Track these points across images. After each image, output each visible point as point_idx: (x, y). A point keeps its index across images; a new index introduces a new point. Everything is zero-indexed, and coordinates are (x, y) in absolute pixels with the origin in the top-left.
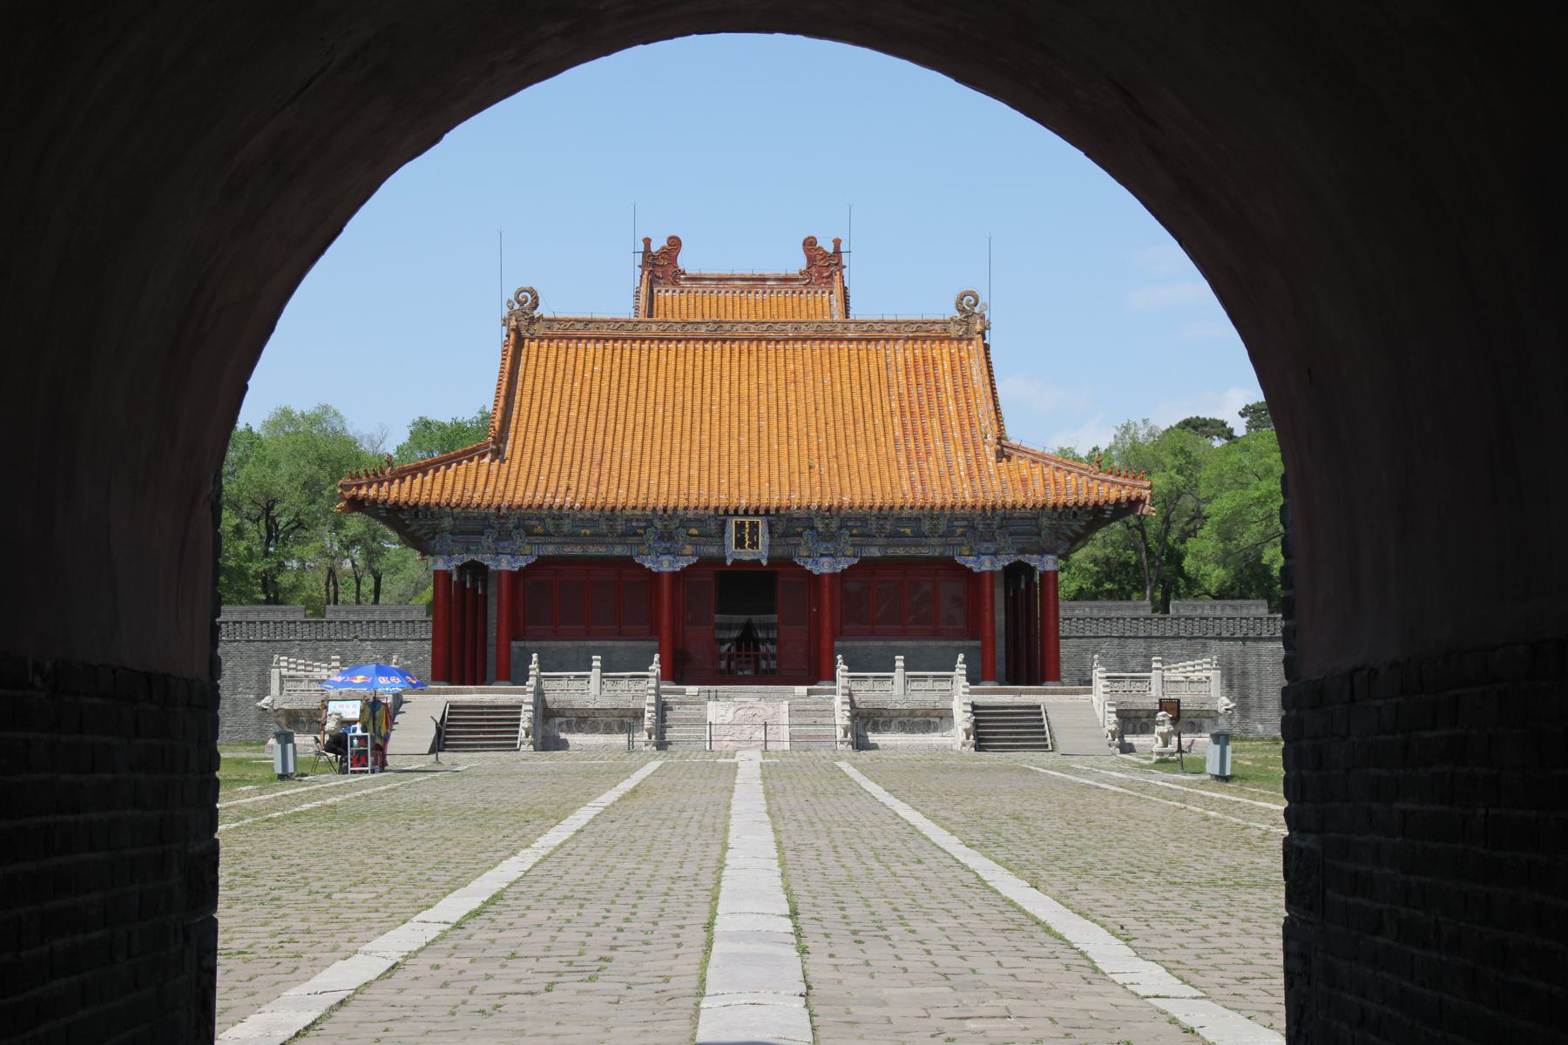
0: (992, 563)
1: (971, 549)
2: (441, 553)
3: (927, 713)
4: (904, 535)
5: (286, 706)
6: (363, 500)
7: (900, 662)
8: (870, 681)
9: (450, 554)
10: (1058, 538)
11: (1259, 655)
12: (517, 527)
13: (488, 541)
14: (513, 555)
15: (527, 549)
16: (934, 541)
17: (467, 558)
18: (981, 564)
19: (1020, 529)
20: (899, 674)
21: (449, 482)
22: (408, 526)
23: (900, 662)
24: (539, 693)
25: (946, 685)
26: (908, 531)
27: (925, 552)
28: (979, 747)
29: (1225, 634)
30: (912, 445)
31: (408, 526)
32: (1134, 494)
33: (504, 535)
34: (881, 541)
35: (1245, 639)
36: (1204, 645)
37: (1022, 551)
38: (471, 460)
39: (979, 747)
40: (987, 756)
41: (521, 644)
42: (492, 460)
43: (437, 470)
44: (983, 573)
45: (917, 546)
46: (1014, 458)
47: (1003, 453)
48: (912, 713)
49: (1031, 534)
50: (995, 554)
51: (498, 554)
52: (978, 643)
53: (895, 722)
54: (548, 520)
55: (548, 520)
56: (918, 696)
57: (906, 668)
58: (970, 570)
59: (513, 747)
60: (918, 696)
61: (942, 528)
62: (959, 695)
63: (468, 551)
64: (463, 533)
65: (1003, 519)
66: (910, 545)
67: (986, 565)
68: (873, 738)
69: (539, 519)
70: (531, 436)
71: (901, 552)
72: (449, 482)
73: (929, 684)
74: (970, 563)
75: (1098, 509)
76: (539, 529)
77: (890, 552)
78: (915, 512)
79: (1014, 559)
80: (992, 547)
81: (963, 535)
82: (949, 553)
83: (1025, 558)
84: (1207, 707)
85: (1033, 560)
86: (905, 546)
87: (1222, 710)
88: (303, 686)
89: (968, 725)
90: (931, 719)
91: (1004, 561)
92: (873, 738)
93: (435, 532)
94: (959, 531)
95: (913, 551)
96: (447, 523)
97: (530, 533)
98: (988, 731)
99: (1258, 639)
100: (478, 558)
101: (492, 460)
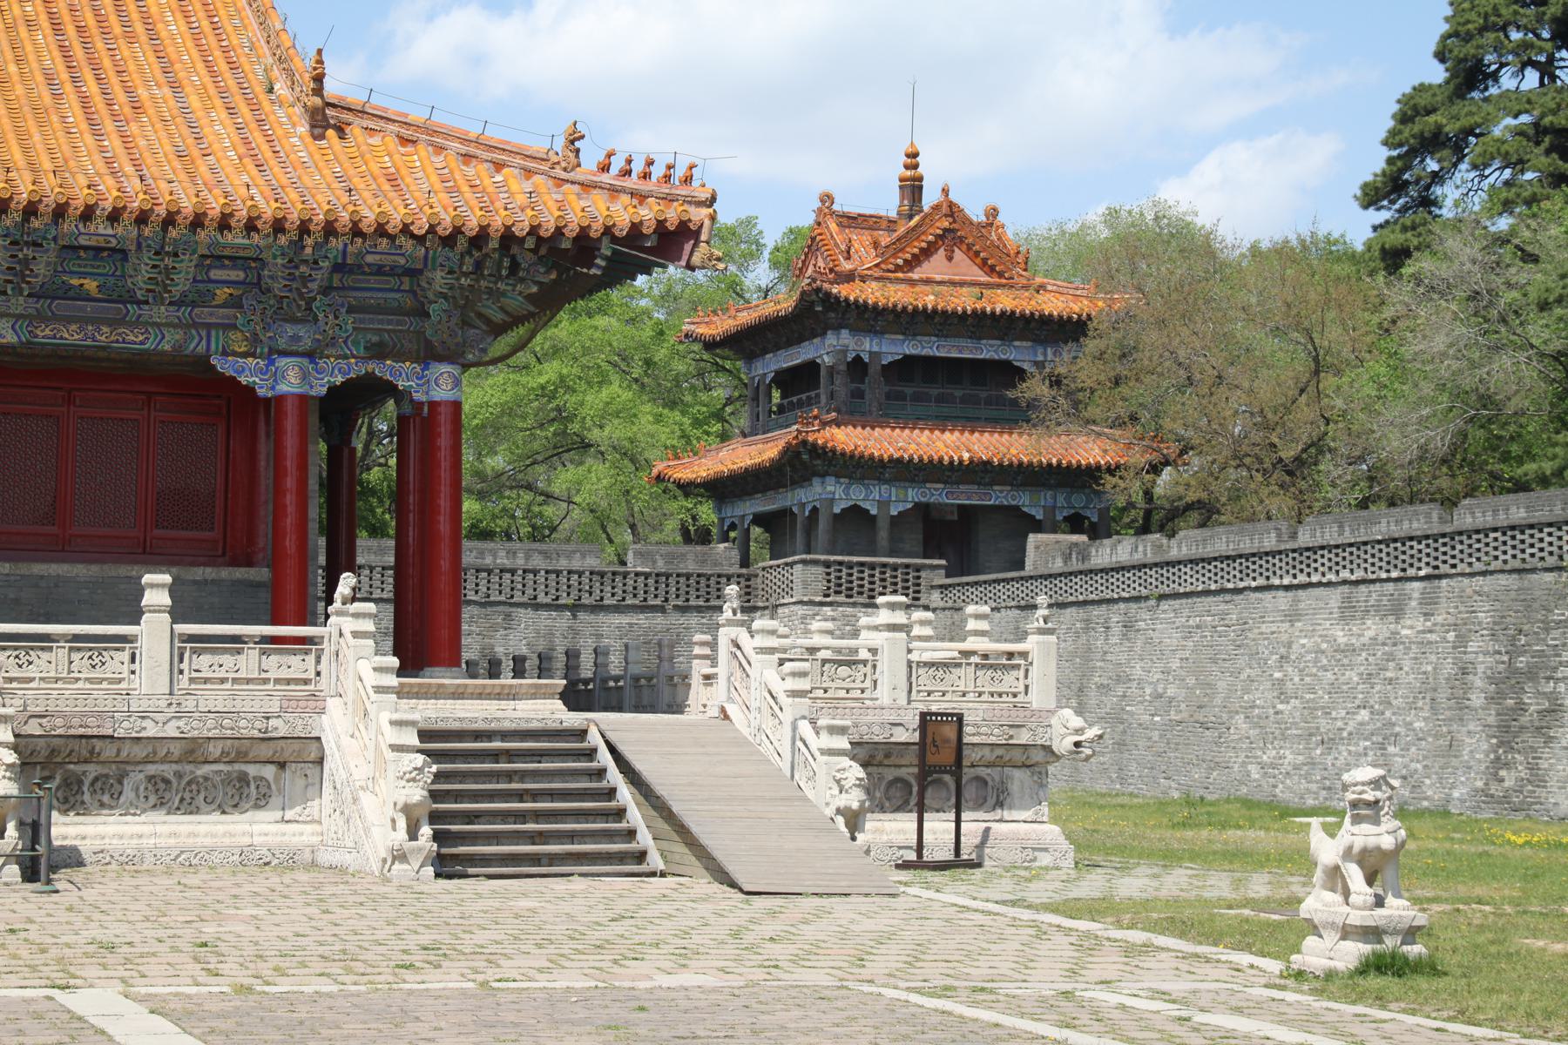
0: (304, 376)
1: (255, 340)
3: (240, 751)
4: (81, 295)
7: (157, 588)
8: (61, 653)
10: (466, 323)
11: (599, 636)
16: (161, 313)
18: (277, 377)
19: (373, 298)
20: (154, 631)
23: (157, 588)
25: (297, 665)
26: (91, 285)
27: (134, 339)
28: (446, 866)
29: (542, 599)
30: (92, 88)
32: (672, 215)
34: (19, 304)
35: (575, 608)
36: (508, 616)
37: (379, 352)
39: (446, 866)
40: (477, 893)
44: (280, 399)
45: (114, 323)
46: (355, 131)
47: (327, 118)
48: (193, 750)
49: (400, 311)
50: (310, 355)
52: (261, 574)
53: (136, 777)
56: (214, 698)
57: (179, 613)
58: (250, 390)
60: (214, 698)
61: (181, 283)
62: (352, 697)
65: (338, 268)
66: (97, 322)
67: (290, 379)
68: (65, 829)
71: (71, 336)
73: (248, 662)
74: (249, 373)
75: (585, 244)
77: (44, 334)
78: (125, 230)
79: (357, 369)
80: (306, 336)
81: (235, 303)
82: (196, 346)
83: (383, 369)
84: (1024, 737)
85: (403, 374)
86: (83, 321)
87: (1063, 745)
89: (416, 794)
90: (251, 769)
91: (332, 374)
92: (65, 829)
94: (223, 293)
95: (104, 336)
98: (484, 815)
99: (598, 608)
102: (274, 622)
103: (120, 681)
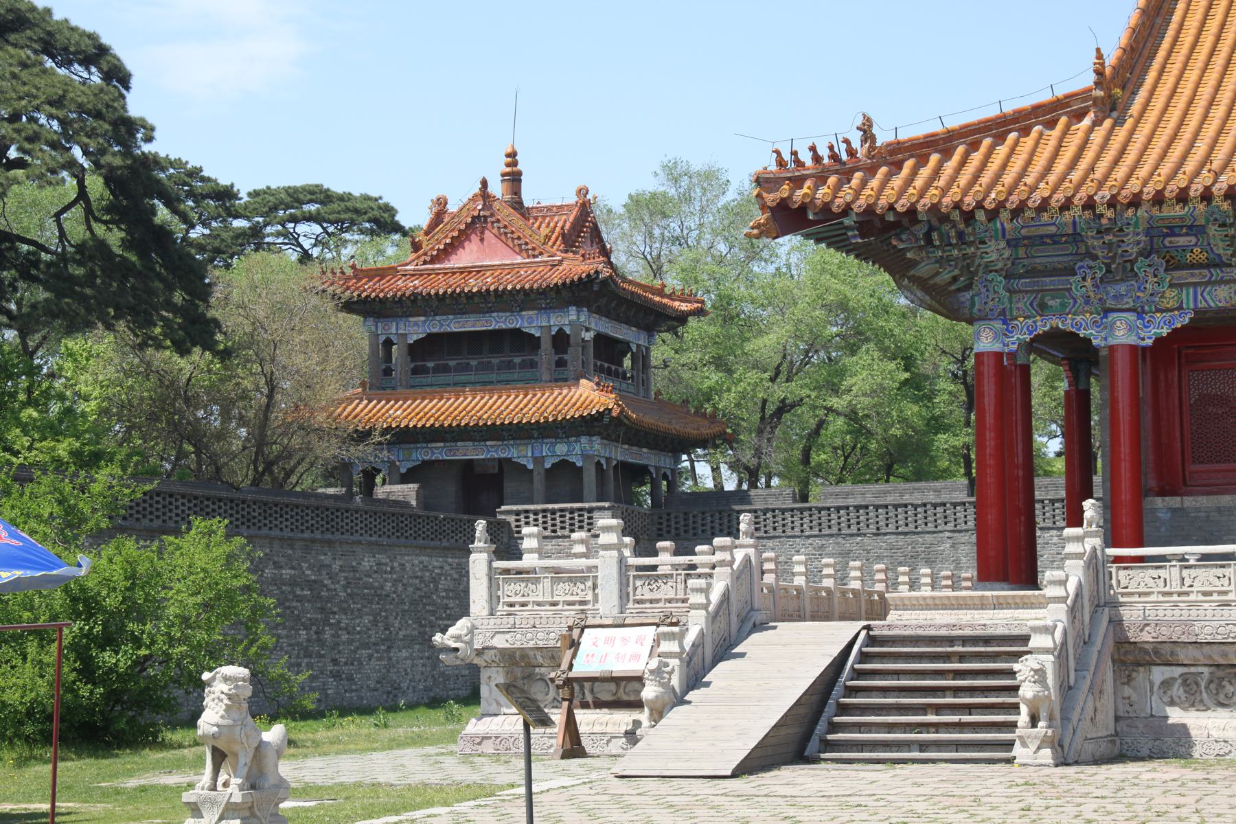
2: (984, 318)
5: (500, 642)
6: (803, 208)
9: (1006, 317)
12: (1145, 253)
13: (1082, 286)
14: (1140, 313)
15: (1171, 297)
17: (1043, 325)
21: (993, 167)
22: (914, 264)
24: (1098, 603)
31: (914, 264)
33: (1119, 269)
38: (1051, 125)
41: (1175, 502)
42: (1097, 123)
43: (974, 146)
51: (1107, 311)
54: (1213, 230)
55: (1213, 230)
59: (999, 750)
63: (1043, 308)
64: (1032, 272)
69: (1196, 230)
70: (1192, 76)
72: (993, 167)
76: (1198, 255)
88: (542, 592)
93: (970, 273)
96: (995, 252)
97: (1174, 264)
100: (1065, 324)
101: (1097, 123)
102: (598, 501)
103: (1225, 593)
